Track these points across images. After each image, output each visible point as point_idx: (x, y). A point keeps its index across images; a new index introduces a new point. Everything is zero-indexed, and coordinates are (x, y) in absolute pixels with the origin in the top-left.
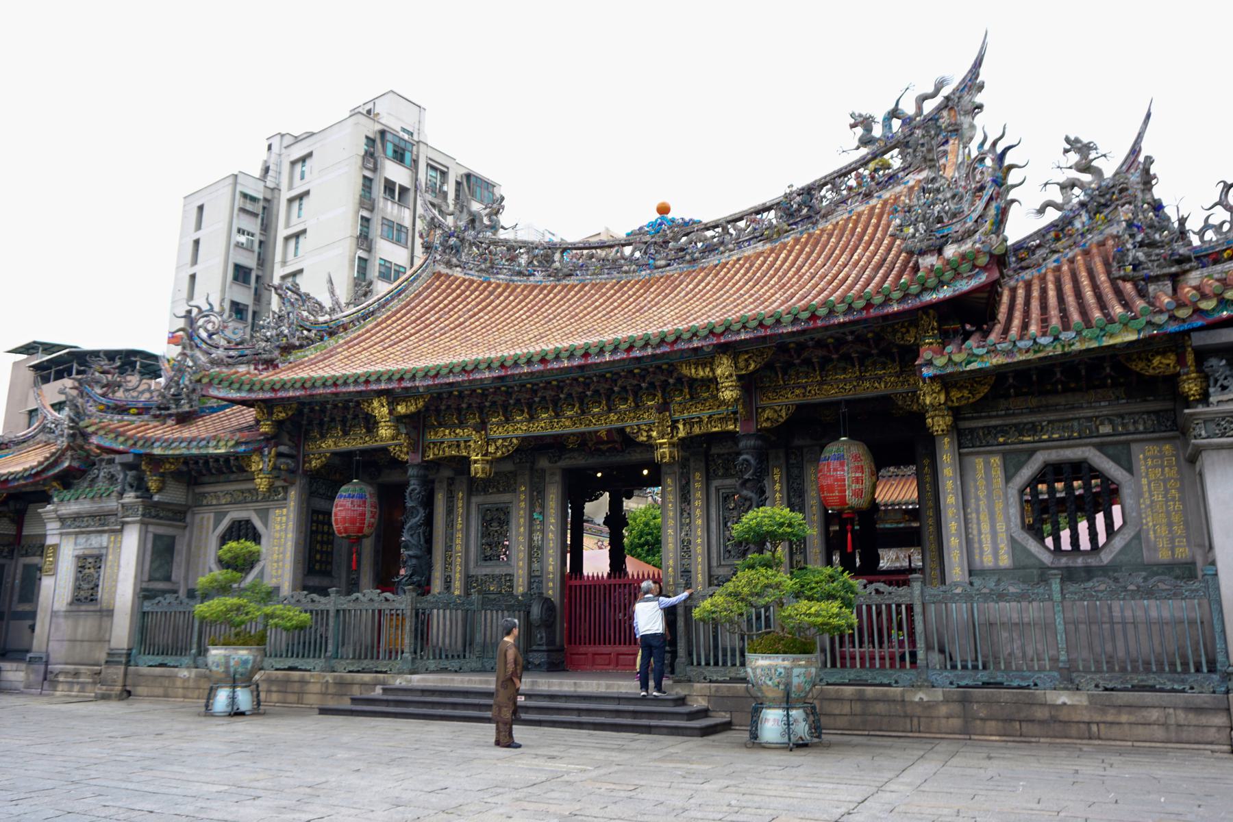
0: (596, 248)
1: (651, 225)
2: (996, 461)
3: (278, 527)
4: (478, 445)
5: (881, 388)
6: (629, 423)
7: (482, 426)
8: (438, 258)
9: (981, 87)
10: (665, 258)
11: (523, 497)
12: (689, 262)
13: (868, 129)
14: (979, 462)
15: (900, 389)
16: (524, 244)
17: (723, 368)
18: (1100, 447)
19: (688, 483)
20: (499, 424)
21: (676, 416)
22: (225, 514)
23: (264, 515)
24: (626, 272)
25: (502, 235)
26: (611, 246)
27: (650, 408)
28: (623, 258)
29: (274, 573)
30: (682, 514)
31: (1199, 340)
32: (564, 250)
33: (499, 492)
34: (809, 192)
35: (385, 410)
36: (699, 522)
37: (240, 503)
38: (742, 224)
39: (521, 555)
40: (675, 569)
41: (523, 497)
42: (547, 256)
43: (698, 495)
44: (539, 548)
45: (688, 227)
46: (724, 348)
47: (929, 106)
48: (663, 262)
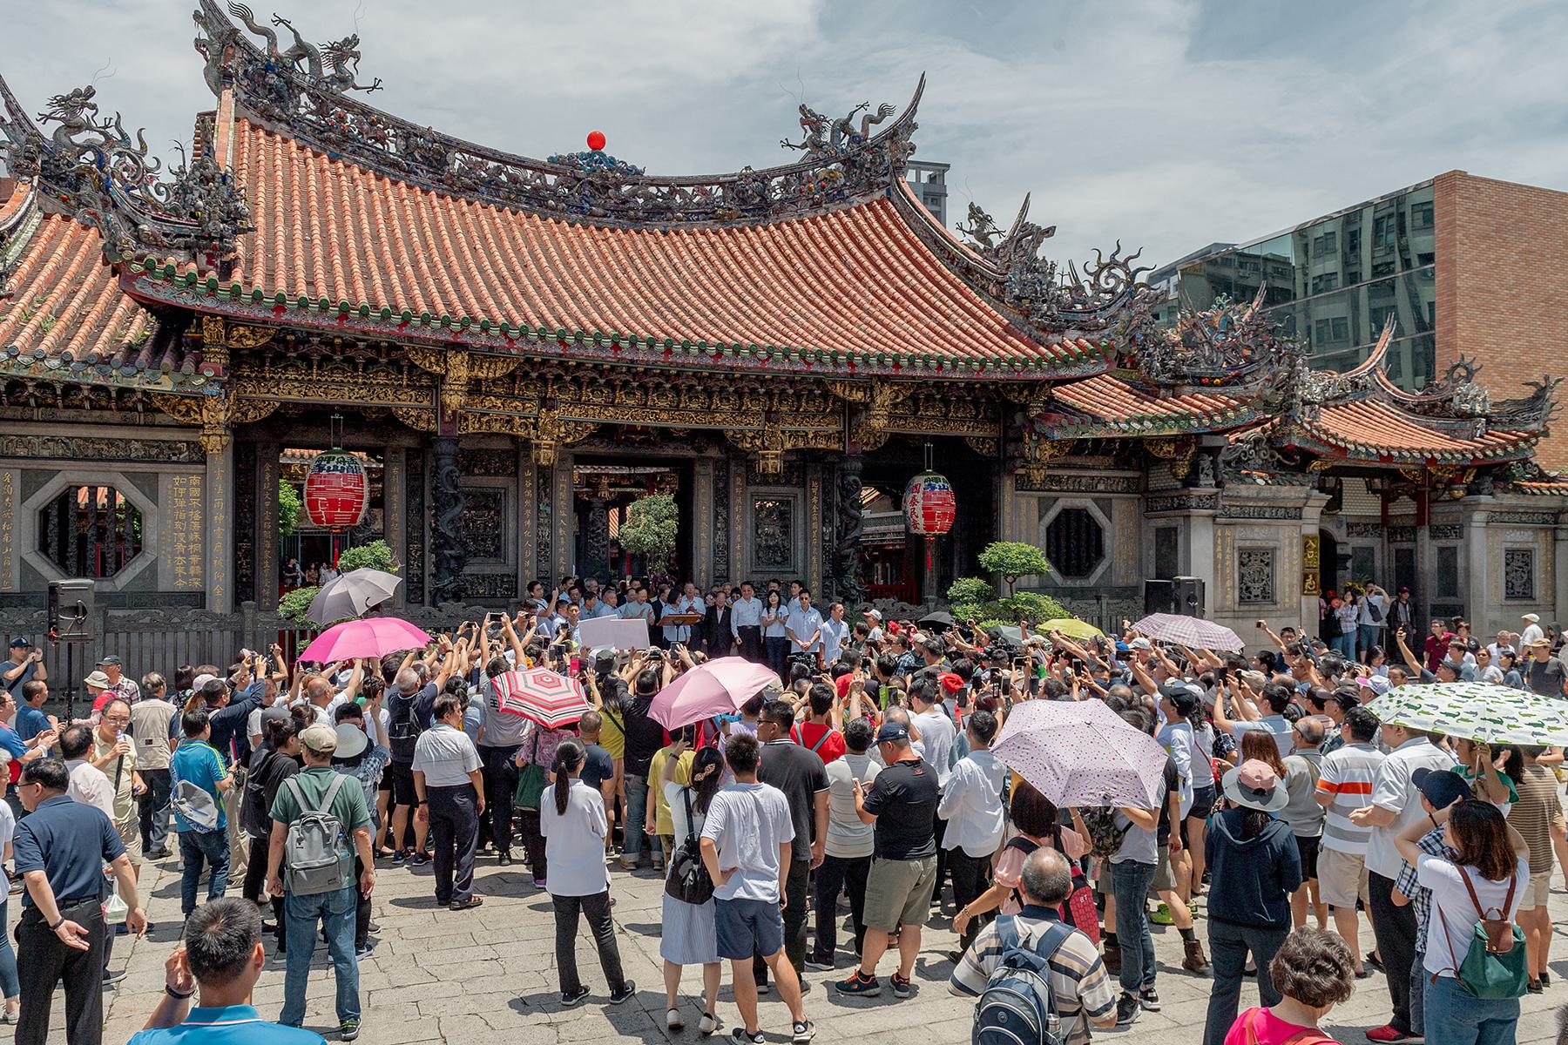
0: (506, 163)
1: (583, 156)
2: (1034, 502)
3: (182, 504)
4: (552, 428)
5: (964, 431)
6: (736, 427)
7: (546, 403)
8: (244, 97)
9: (915, 127)
10: (598, 206)
11: (528, 484)
12: (630, 219)
13: (818, 131)
14: (1023, 501)
15: (977, 433)
16: (399, 125)
17: (884, 396)
18: (1096, 500)
19: (727, 484)
20: (577, 402)
21: (787, 427)
22: (52, 474)
23: (149, 486)
24: (552, 209)
25: (349, 93)
26: (526, 167)
27: (757, 413)
28: (547, 188)
29: (180, 570)
30: (716, 518)
31: (1208, 442)
32: (461, 151)
33: (488, 473)
34: (764, 177)
35: (464, 373)
36: (739, 528)
37: (86, 459)
38: (689, 190)
39: (528, 554)
40: (708, 575)
41: (528, 484)
42: (439, 153)
43: (739, 500)
44: (547, 545)
45: (633, 175)
46: (884, 379)
47: (874, 131)
48: (601, 211)
